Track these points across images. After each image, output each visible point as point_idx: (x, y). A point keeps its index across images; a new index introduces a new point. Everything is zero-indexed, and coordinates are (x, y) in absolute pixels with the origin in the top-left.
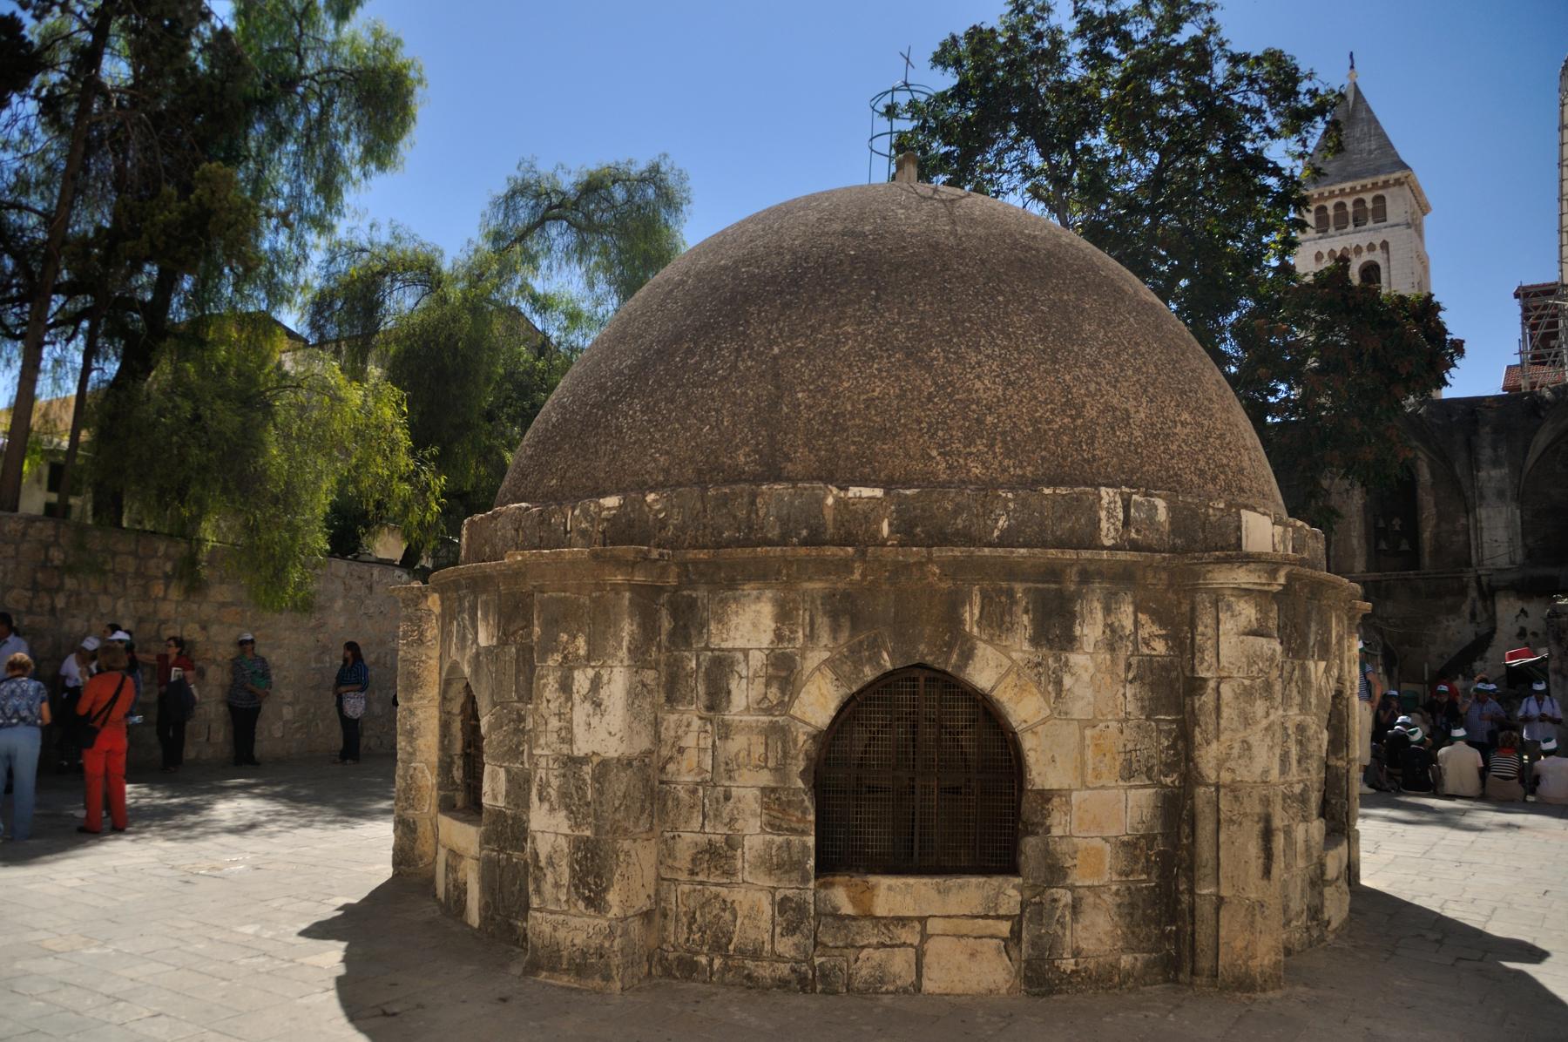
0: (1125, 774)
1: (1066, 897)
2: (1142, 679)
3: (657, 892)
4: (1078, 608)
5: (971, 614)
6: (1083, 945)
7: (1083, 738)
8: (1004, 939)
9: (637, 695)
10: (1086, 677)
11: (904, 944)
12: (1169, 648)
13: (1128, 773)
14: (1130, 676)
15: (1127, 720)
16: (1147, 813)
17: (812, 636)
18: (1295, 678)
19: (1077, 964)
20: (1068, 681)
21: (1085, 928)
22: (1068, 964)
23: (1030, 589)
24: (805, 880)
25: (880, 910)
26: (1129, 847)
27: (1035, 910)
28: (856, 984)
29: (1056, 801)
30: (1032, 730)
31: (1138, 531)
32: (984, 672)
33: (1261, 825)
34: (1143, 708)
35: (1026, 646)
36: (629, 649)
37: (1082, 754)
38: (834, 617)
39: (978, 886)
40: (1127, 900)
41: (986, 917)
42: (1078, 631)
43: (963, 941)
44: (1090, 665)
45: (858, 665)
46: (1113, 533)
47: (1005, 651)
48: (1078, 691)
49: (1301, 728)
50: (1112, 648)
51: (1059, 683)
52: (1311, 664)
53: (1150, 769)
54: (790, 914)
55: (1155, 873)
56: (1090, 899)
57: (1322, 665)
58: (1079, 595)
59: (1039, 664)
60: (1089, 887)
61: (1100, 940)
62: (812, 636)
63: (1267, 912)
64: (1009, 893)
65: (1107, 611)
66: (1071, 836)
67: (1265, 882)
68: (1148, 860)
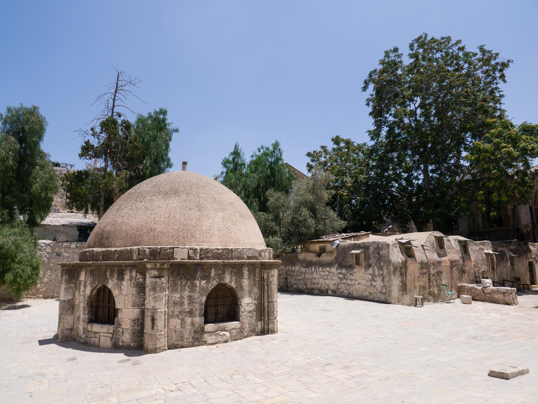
0: (133, 306)
1: (121, 330)
2: (137, 286)
3: (73, 325)
4: (125, 272)
5: (108, 274)
6: (124, 340)
7: (125, 298)
8: (111, 338)
9: (67, 289)
10: (126, 286)
11: (97, 337)
12: (143, 280)
13: (134, 306)
14: (134, 286)
15: (133, 295)
16: (138, 314)
17: (88, 278)
19: (122, 344)
20: (122, 287)
21: (124, 337)
22: (121, 344)
23: (116, 269)
24: (86, 324)
25: (94, 331)
26: (134, 321)
27: (115, 332)
28: (91, 344)
29: (120, 311)
30: (116, 296)
31: (141, 256)
32: (110, 286)
33: (151, 318)
34: (137, 292)
35: (116, 280)
36: (65, 281)
37: (125, 301)
38: (90, 274)
39: (107, 327)
40: (133, 332)
41: (108, 333)
42: (124, 277)
43: (105, 337)
44: (126, 283)
45: (93, 284)
46: (135, 257)
47: (113, 281)
48: (124, 289)
50: (131, 280)
51: (121, 287)
52: (198, 282)
53: (138, 305)
54: (85, 331)
55: (139, 327)
56: (125, 331)
57: (203, 282)
58: (125, 270)
59: (118, 284)
60: (125, 329)
61: (127, 339)
62: (88, 278)
63: (152, 337)
64: (111, 328)
65: (130, 273)
66: (122, 318)
67: (152, 330)
68: (138, 324)
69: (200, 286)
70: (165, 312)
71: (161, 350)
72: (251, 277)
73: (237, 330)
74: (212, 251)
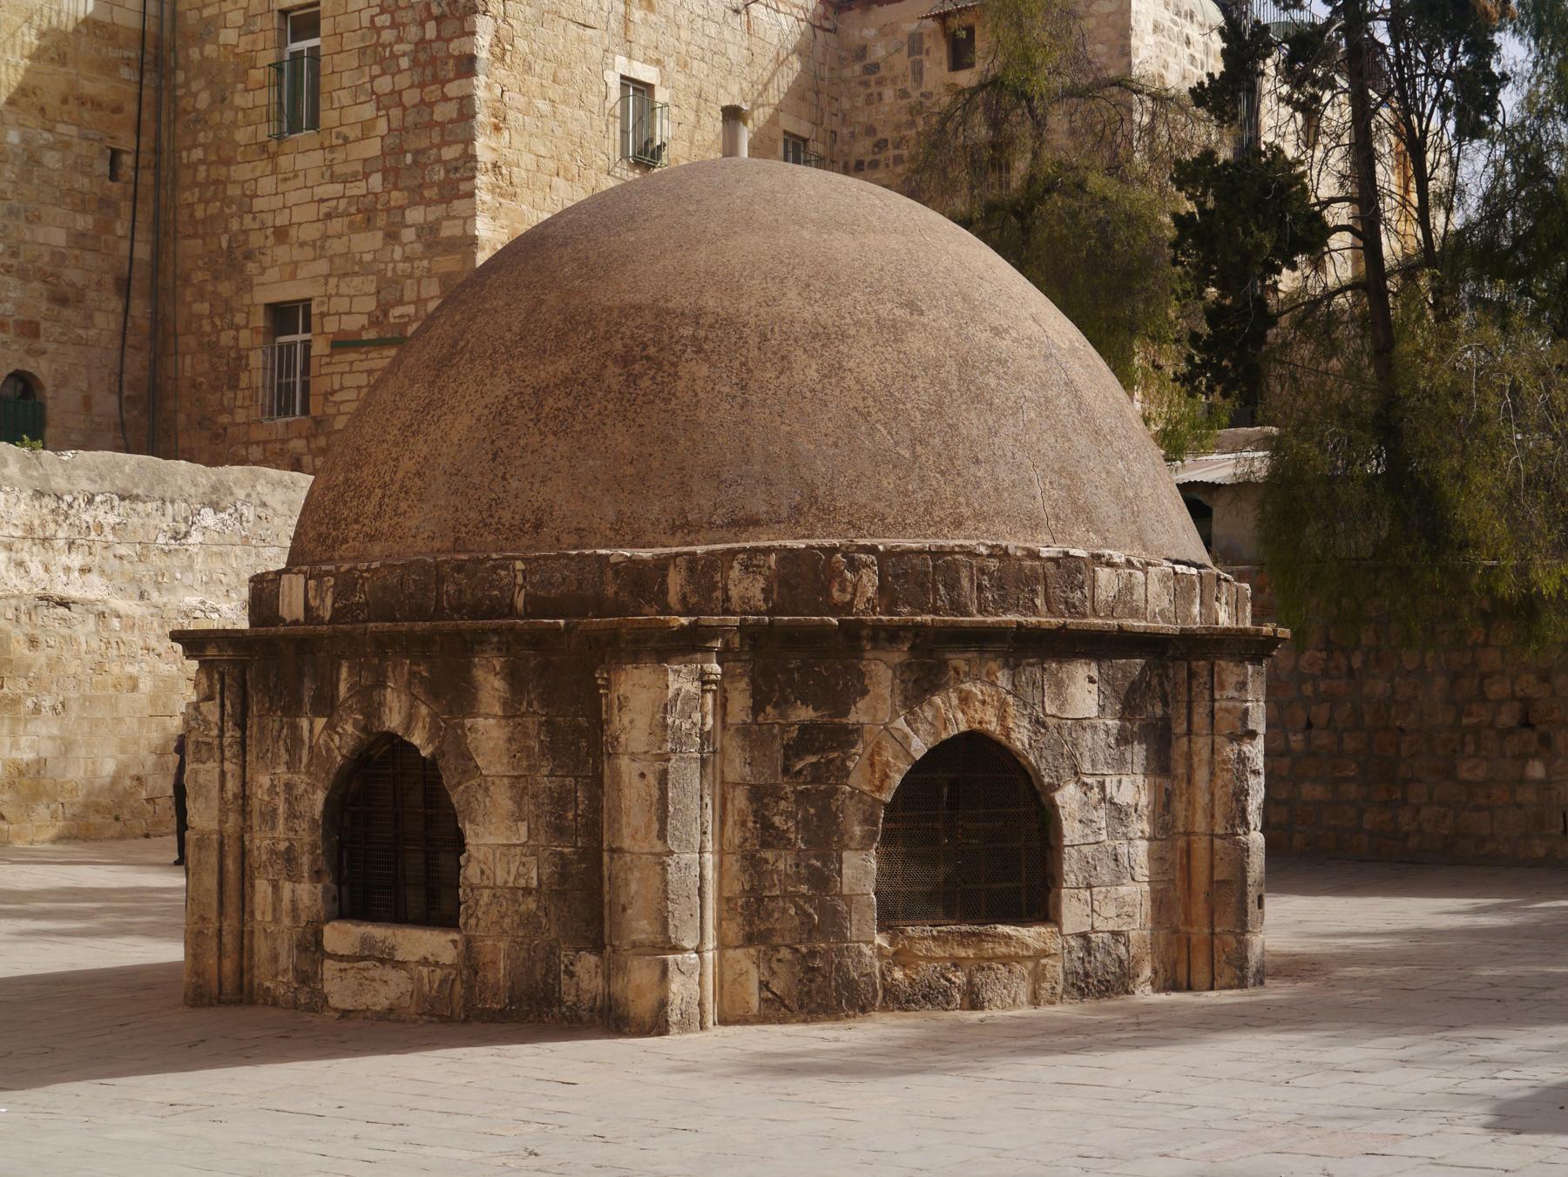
18: (283, 736)
49: (289, 787)
52: (305, 723)
57: (320, 722)
69: (311, 741)
70: (221, 844)
71: (206, 1000)
72: (523, 709)
73: (439, 973)
74: (367, 579)
